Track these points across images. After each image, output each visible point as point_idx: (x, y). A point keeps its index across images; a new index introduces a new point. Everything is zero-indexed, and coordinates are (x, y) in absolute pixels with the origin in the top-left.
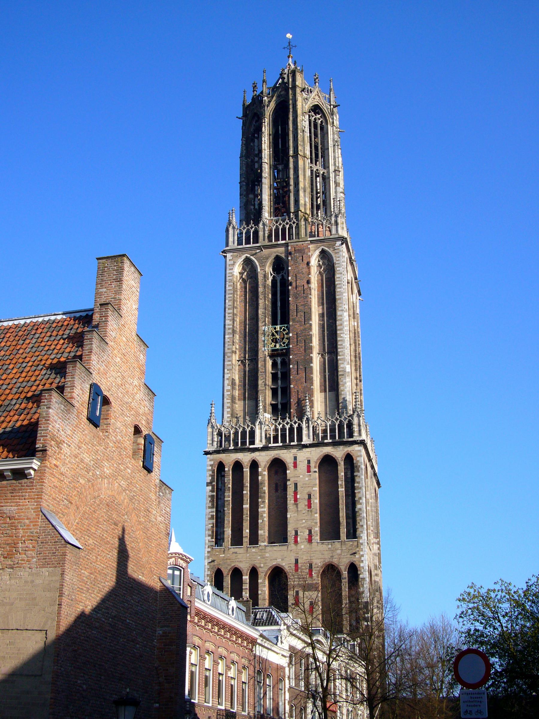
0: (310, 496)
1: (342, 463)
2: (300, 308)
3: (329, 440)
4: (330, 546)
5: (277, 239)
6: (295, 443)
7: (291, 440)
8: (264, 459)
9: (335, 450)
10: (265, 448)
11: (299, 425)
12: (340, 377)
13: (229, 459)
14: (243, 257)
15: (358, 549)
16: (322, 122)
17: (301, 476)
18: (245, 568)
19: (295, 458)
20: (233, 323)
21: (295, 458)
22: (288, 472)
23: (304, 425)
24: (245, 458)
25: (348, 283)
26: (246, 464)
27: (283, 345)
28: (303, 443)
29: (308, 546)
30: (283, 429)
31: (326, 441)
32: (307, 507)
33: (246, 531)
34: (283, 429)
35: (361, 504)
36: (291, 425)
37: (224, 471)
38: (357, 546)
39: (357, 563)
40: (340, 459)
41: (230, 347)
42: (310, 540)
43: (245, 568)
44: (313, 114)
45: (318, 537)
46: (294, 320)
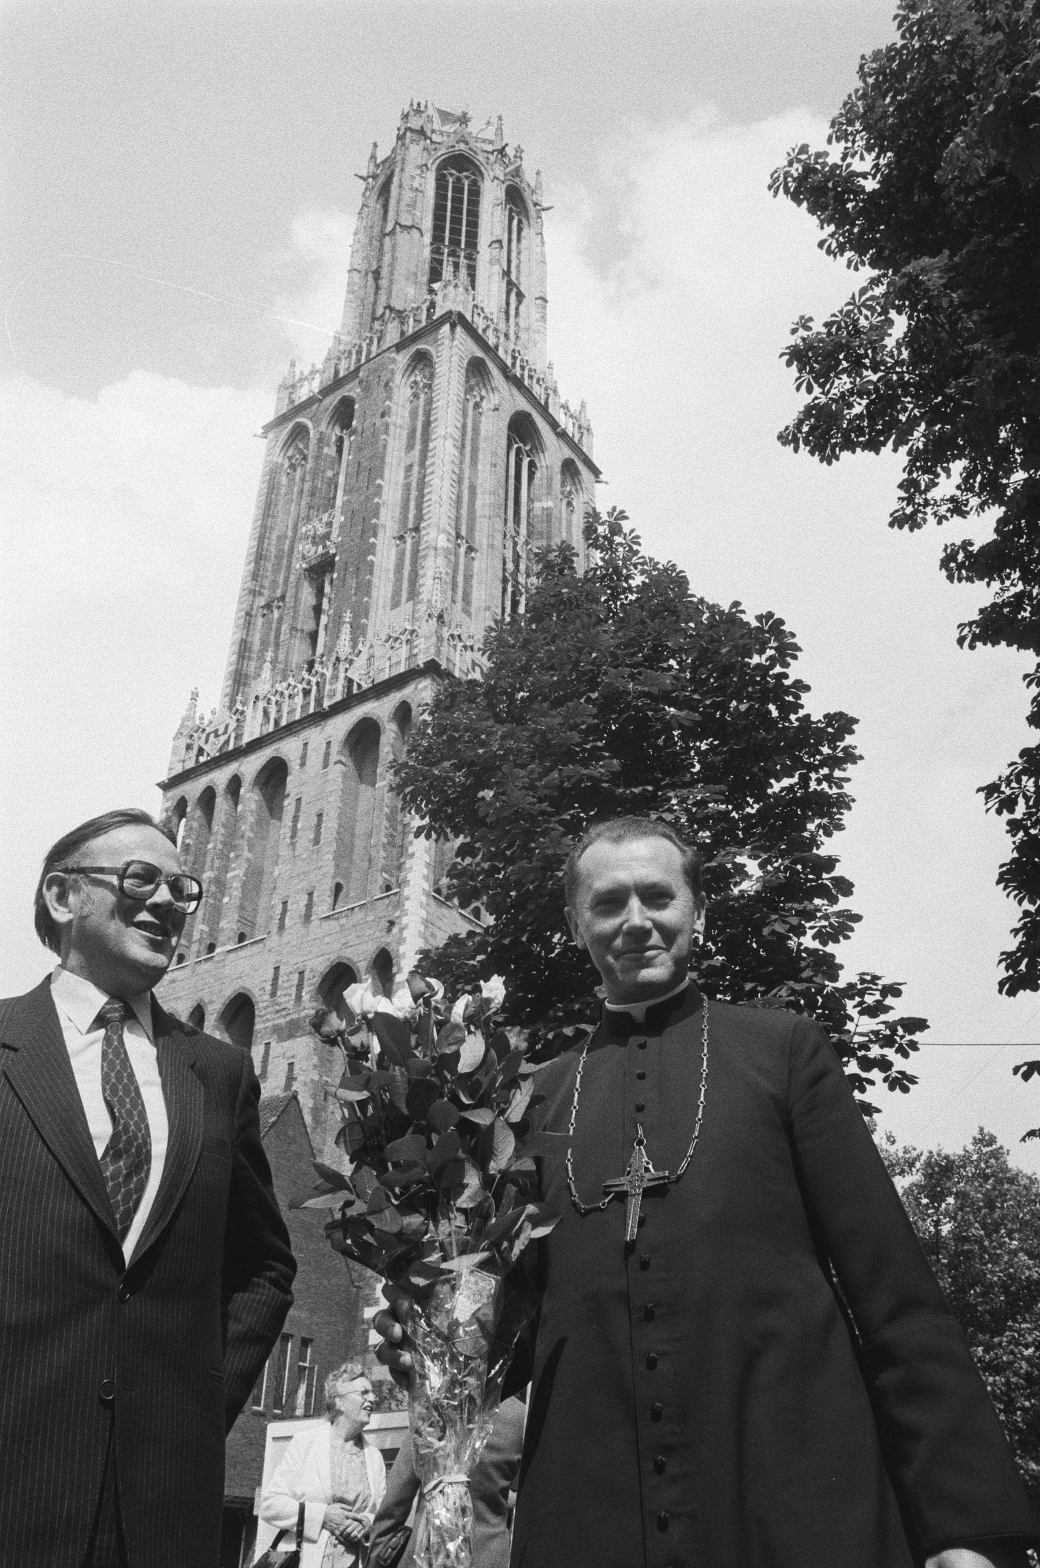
8: (250, 767)
14: (291, 425)
15: (397, 914)
22: (289, 779)
24: (220, 778)
29: (303, 931)
39: (390, 949)
42: (307, 917)
44: (454, 172)
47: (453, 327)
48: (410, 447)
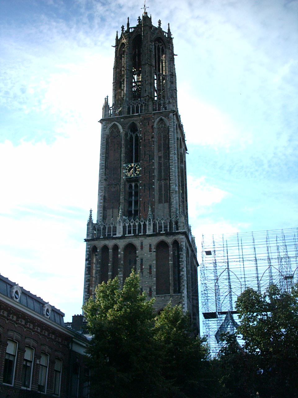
0: (150, 266)
1: (171, 246)
2: (147, 152)
3: (163, 232)
4: (163, 298)
5: (133, 113)
6: (142, 234)
7: (140, 232)
8: (122, 244)
9: (167, 238)
10: (123, 237)
11: (145, 222)
12: (171, 194)
13: (100, 244)
14: (113, 123)
15: (181, 300)
16: (162, 47)
17: (145, 254)
19: (142, 243)
20: (106, 162)
21: (142, 243)
22: (137, 252)
23: (147, 223)
24: (110, 243)
25: (178, 139)
26: (110, 247)
27: (136, 175)
28: (147, 234)
30: (134, 226)
31: (161, 232)
32: (148, 274)
34: (134, 226)
35: (183, 271)
36: (140, 223)
37: (97, 252)
38: (181, 299)
40: (170, 243)
41: (103, 177)
44: (157, 42)
45: (155, 293)
46: (143, 160)
47: (174, 115)
48: (159, 150)
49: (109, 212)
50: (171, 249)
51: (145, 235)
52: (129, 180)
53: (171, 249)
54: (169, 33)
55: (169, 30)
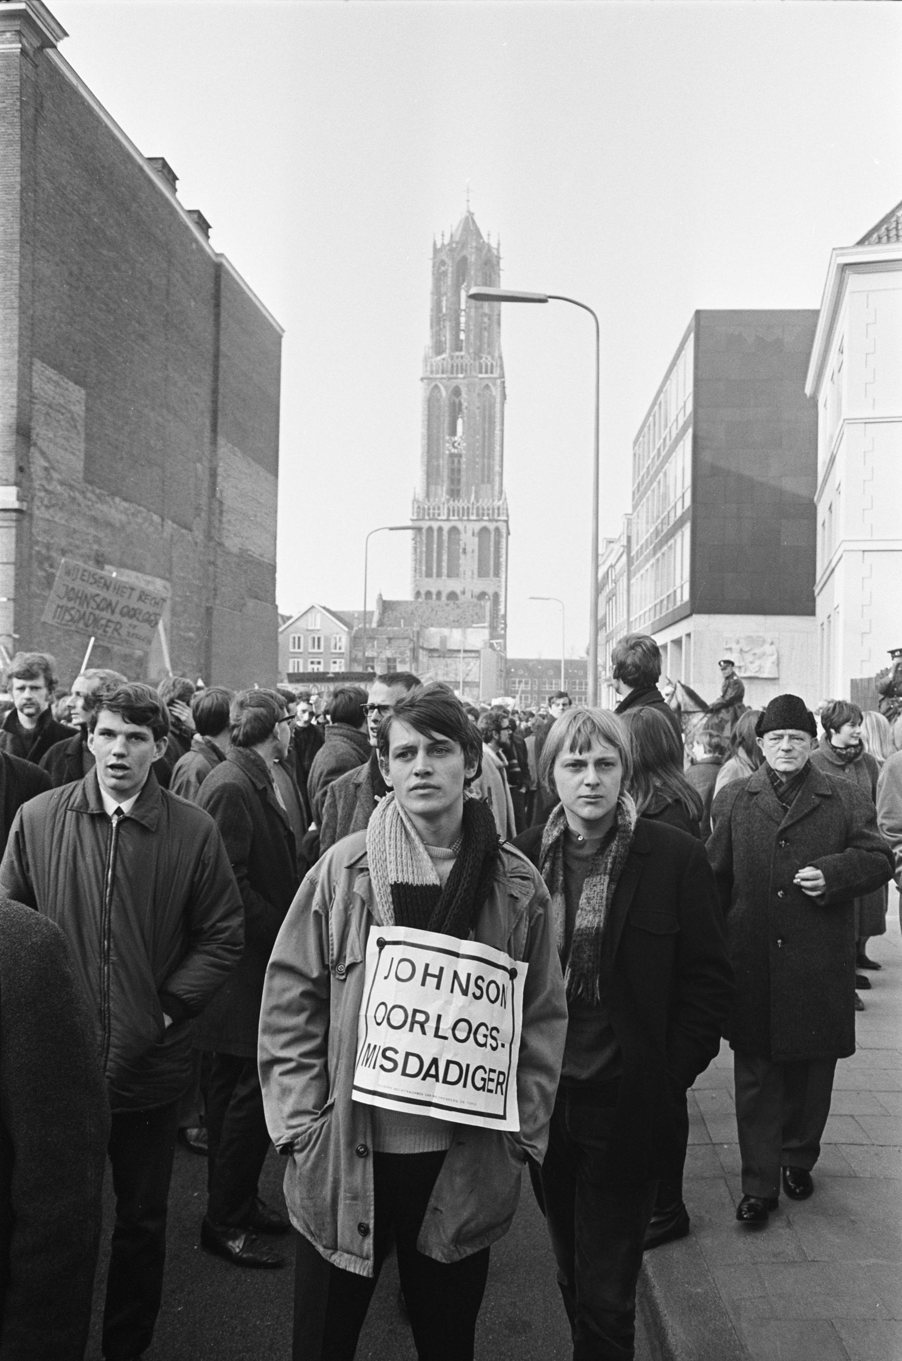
0: (473, 552)
8: (446, 526)
10: (448, 520)
18: (434, 591)
33: (435, 570)
42: (473, 578)
43: (434, 591)
49: (432, 488)
50: (492, 535)
51: (469, 520)
52: (452, 455)
53: (492, 535)
54: (498, 249)
55: (499, 244)
